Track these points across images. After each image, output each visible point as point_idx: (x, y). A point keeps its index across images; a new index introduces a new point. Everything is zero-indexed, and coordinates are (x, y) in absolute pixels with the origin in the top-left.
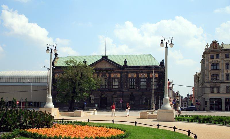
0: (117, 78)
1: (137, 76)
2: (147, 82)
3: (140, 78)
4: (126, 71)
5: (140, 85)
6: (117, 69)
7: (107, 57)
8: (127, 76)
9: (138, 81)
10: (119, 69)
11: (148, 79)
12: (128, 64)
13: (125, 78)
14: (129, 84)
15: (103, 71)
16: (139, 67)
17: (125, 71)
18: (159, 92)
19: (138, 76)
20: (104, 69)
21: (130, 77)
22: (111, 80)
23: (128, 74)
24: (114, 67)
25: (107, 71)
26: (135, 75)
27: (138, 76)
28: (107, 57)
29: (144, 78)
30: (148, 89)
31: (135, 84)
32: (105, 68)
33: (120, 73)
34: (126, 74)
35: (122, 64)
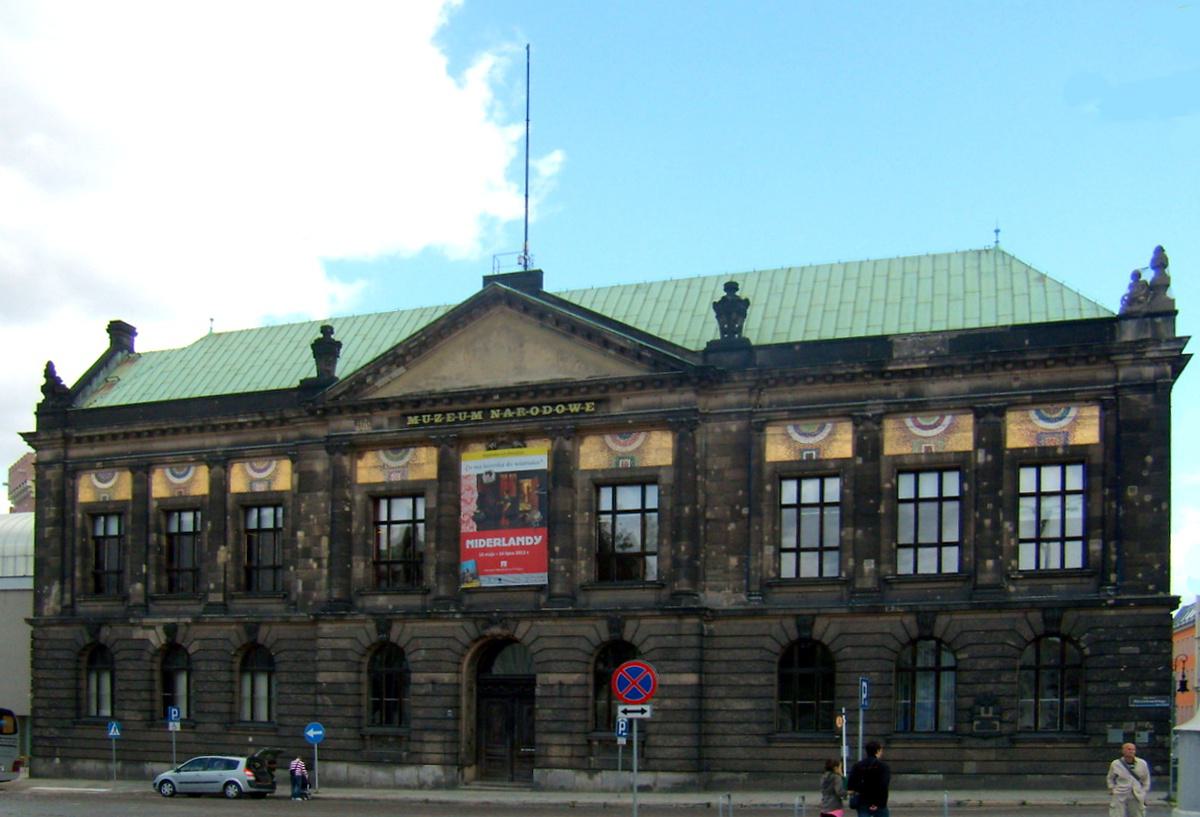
0: (642, 479)
1: (859, 447)
2: (978, 504)
3: (901, 467)
4: (740, 405)
5: (894, 535)
6: (640, 384)
7: (538, 275)
8: (748, 449)
9: (877, 492)
10: (658, 384)
11: (980, 471)
12: (758, 329)
13: (728, 474)
14: (776, 537)
15: (495, 414)
16: (880, 346)
17: (732, 398)
18: (1119, 604)
19: (868, 446)
20: (505, 392)
21: (775, 463)
22: (580, 496)
23: (760, 428)
24: (615, 368)
25: (534, 411)
26: (841, 444)
27: (868, 446)
28: (538, 275)
29: (939, 465)
30: (985, 578)
31: (842, 525)
32: (511, 380)
33: (682, 425)
34: (734, 427)
35: (696, 331)
